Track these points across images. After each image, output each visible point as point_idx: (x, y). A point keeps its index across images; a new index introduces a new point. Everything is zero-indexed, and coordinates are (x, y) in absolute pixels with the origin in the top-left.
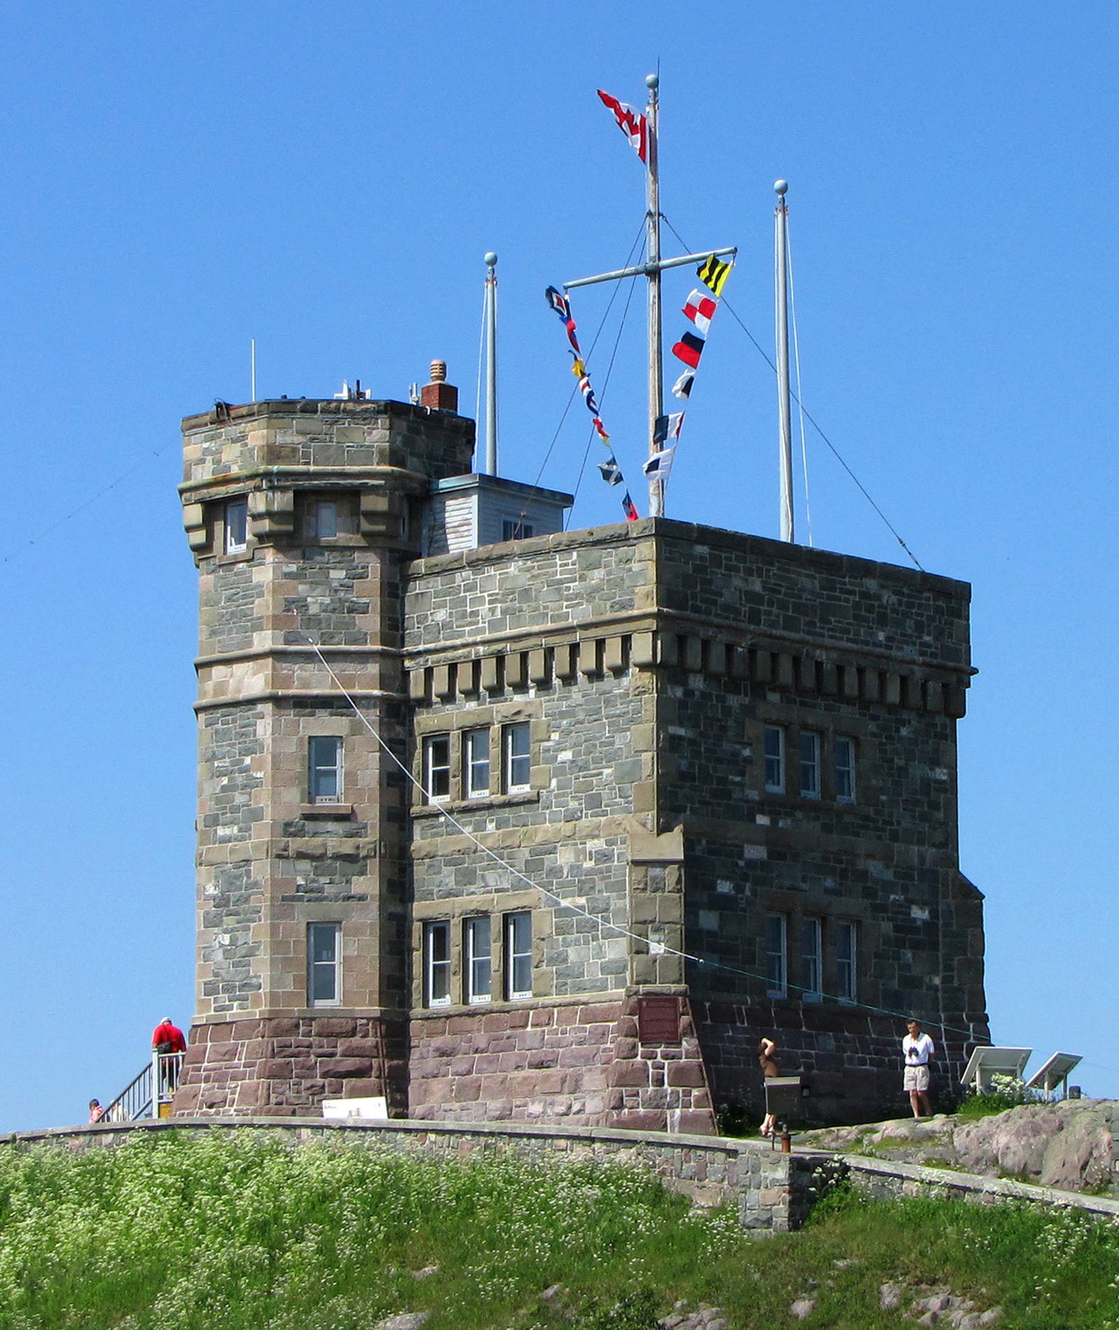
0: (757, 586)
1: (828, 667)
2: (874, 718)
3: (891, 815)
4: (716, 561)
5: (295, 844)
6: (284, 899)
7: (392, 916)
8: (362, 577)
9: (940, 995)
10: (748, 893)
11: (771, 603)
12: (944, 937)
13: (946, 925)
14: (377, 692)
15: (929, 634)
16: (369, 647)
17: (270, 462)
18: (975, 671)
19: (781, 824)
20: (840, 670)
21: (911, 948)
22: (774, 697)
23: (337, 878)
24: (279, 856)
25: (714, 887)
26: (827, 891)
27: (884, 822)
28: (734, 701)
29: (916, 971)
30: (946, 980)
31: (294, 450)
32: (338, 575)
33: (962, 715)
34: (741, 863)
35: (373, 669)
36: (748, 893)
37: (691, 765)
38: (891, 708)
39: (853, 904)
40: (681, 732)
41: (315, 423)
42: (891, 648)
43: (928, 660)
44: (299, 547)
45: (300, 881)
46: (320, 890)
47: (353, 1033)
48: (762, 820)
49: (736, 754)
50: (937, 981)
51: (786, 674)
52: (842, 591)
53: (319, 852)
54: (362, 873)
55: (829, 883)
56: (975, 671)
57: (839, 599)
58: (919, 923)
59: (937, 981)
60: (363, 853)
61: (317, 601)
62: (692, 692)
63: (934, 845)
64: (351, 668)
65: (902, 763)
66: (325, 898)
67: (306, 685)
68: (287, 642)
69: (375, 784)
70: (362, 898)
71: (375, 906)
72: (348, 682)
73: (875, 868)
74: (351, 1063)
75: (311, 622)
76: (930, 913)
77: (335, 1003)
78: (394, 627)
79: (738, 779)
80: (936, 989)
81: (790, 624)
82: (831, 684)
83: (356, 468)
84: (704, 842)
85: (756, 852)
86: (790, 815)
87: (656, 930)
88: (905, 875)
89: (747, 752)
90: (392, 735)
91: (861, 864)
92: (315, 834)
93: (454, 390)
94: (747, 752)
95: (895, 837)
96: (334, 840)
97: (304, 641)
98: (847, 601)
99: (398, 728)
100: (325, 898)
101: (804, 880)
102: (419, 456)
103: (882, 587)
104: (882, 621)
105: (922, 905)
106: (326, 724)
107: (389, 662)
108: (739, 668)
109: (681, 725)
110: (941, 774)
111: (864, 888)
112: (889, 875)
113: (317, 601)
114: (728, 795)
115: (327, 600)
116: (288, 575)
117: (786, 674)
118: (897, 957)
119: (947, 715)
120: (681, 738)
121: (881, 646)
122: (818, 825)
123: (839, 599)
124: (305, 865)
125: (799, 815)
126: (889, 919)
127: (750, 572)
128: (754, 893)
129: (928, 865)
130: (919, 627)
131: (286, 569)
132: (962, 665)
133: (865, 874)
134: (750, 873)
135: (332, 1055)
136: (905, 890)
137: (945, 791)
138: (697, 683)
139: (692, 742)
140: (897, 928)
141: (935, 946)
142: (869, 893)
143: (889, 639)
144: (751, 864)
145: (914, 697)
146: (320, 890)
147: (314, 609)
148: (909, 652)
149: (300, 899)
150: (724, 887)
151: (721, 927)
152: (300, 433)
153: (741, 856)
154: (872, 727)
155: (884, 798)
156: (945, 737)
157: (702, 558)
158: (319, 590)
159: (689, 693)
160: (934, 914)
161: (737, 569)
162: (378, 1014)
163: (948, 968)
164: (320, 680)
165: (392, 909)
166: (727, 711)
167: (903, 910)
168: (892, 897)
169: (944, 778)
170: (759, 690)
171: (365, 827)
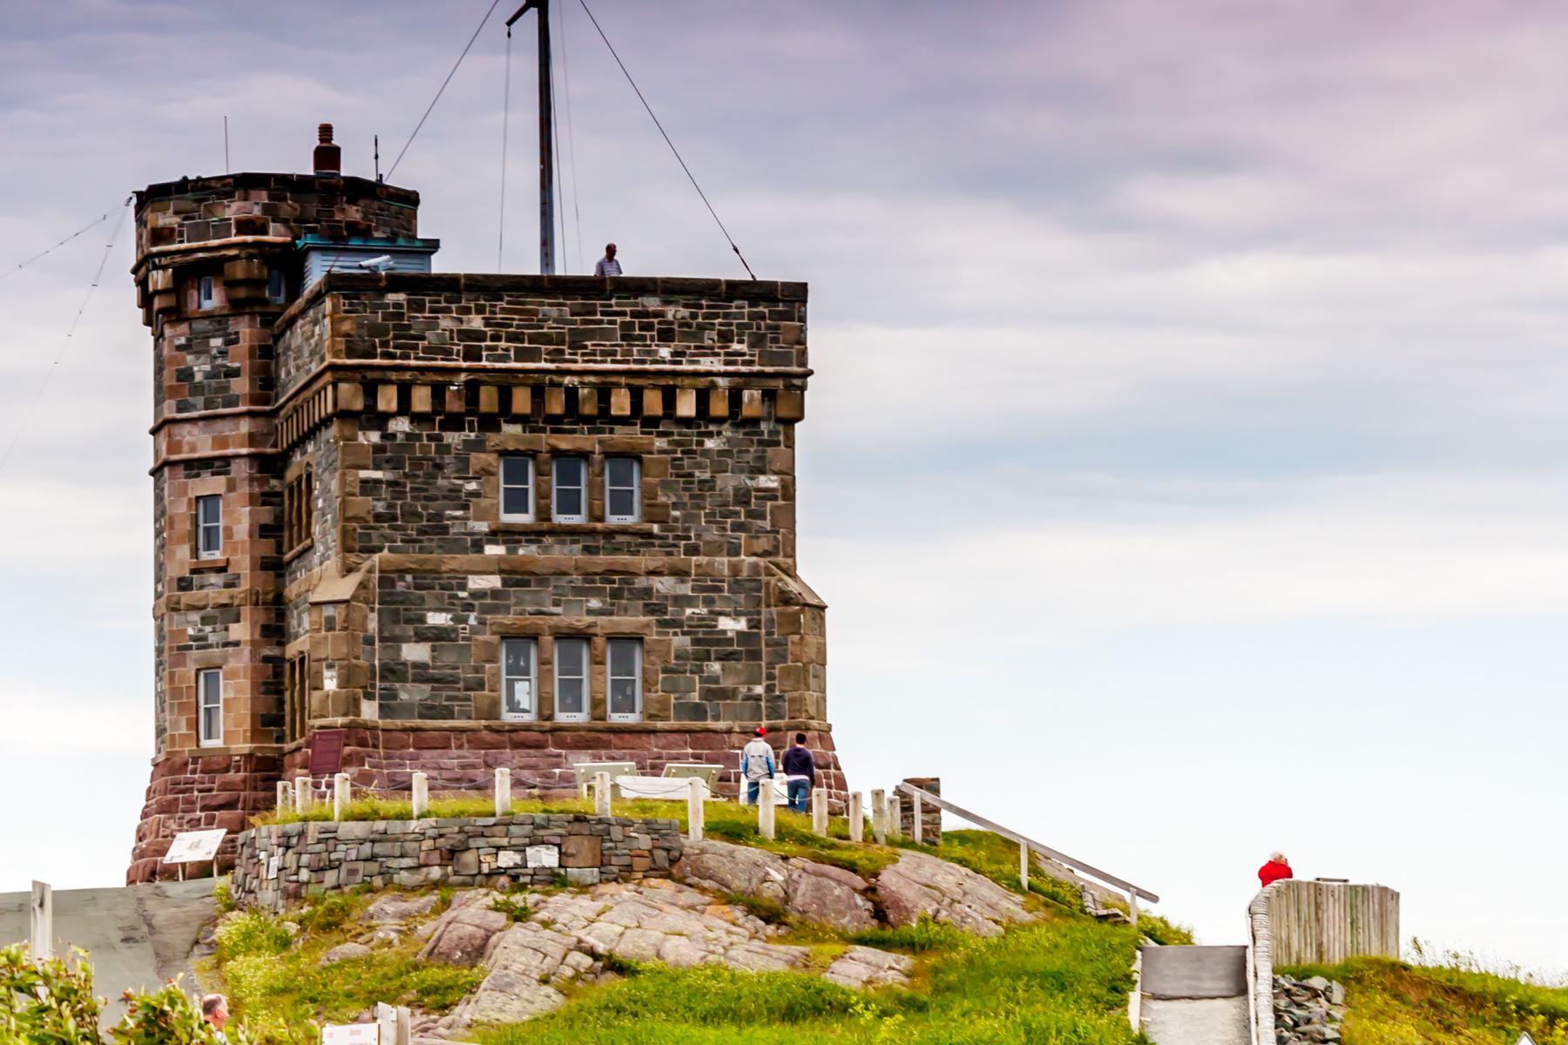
0: (476, 322)
1: (583, 392)
2: (661, 435)
3: (688, 530)
4: (420, 307)
5: (186, 598)
6: (179, 648)
7: (266, 659)
8: (236, 341)
9: (763, 704)
10: (472, 621)
11: (496, 338)
12: (767, 645)
13: (769, 633)
14: (244, 451)
15: (741, 342)
16: (242, 408)
17: (154, 244)
18: (811, 373)
19: (521, 552)
20: (604, 393)
21: (718, 659)
22: (516, 429)
23: (218, 626)
24: (173, 610)
25: (422, 620)
26: (590, 612)
27: (677, 537)
28: (453, 438)
29: (727, 683)
30: (769, 689)
31: (172, 230)
32: (216, 342)
33: (800, 418)
34: (463, 594)
35: (245, 426)
36: (472, 621)
37: (390, 506)
38: (686, 422)
39: (631, 620)
40: (378, 475)
41: (187, 203)
42: (680, 363)
43: (731, 368)
44: (186, 319)
45: (191, 631)
46: (205, 638)
47: (227, 770)
48: (494, 550)
49: (457, 490)
50: (759, 690)
51: (522, 401)
52: (603, 314)
53: (202, 603)
54: (237, 620)
55: (595, 603)
56: (811, 373)
57: (601, 322)
58: (730, 634)
59: (759, 690)
60: (236, 602)
61: (201, 368)
62: (394, 436)
63: (755, 554)
64: (225, 428)
65: (707, 476)
66: (210, 646)
67: (193, 449)
68: (179, 410)
69: (246, 537)
70: (236, 644)
71: (246, 650)
72: (221, 442)
73: (664, 585)
74: (224, 796)
75: (197, 389)
76: (749, 621)
77: (217, 743)
78: (266, 383)
79: (459, 513)
80: (758, 698)
81: (522, 355)
82: (588, 409)
83: (215, 242)
84: (409, 578)
85: (495, 582)
86: (539, 542)
87: (330, 667)
88: (709, 588)
89: (472, 486)
90: (266, 489)
91: (641, 582)
92: (202, 587)
93: (337, 150)
94: (472, 486)
95: (693, 550)
96: (213, 590)
97: (193, 407)
98: (610, 322)
99: (273, 482)
100: (210, 646)
101: (556, 604)
102: (285, 222)
103: (666, 303)
104: (666, 336)
105: (737, 614)
106: (211, 484)
107: (261, 421)
108: (454, 405)
109: (377, 467)
110: (768, 481)
111: (646, 605)
112: (686, 589)
113: (201, 368)
114: (445, 530)
115: (208, 368)
116: (180, 348)
117: (522, 401)
118: (700, 670)
119: (779, 420)
120: (377, 481)
121: (664, 362)
122: (578, 547)
123: (601, 322)
124: (195, 617)
125: (548, 540)
126: (684, 633)
127: (467, 311)
128: (482, 622)
129: (745, 574)
130: (726, 337)
131: (177, 342)
132: (795, 369)
133: (648, 592)
134: (476, 603)
135: (210, 790)
136: (709, 602)
137: (775, 498)
138: (401, 426)
139: (390, 484)
140: (696, 642)
141: (755, 655)
142: (650, 609)
143: (674, 354)
144: (478, 595)
145: (719, 407)
146: (205, 638)
147: (198, 378)
148: (706, 364)
149: (190, 648)
150: (437, 619)
151: (434, 658)
152: (176, 213)
153: (463, 587)
154: (660, 443)
155: (676, 513)
156: (777, 443)
157: (397, 305)
158: (203, 358)
159: (386, 436)
160: (754, 624)
161: (447, 310)
162: (247, 751)
163: (770, 677)
164: (199, 442)
165: (267, 652)
166: (444, 449)
167: (707, 623)
168: (689, 611)
169: (775, 485)
170: (490, 423)
171: (238, 576)
